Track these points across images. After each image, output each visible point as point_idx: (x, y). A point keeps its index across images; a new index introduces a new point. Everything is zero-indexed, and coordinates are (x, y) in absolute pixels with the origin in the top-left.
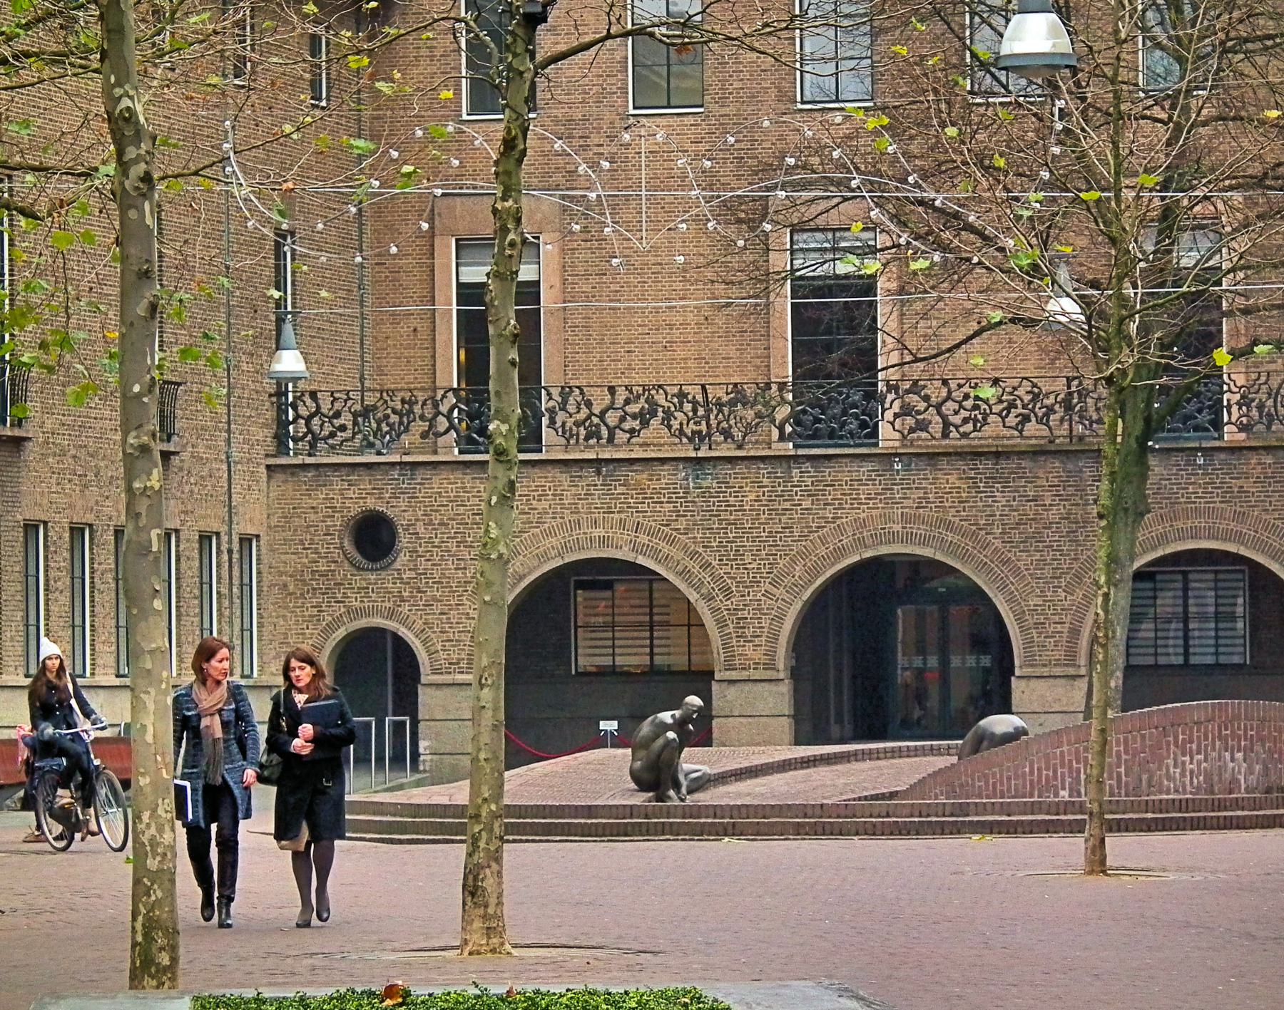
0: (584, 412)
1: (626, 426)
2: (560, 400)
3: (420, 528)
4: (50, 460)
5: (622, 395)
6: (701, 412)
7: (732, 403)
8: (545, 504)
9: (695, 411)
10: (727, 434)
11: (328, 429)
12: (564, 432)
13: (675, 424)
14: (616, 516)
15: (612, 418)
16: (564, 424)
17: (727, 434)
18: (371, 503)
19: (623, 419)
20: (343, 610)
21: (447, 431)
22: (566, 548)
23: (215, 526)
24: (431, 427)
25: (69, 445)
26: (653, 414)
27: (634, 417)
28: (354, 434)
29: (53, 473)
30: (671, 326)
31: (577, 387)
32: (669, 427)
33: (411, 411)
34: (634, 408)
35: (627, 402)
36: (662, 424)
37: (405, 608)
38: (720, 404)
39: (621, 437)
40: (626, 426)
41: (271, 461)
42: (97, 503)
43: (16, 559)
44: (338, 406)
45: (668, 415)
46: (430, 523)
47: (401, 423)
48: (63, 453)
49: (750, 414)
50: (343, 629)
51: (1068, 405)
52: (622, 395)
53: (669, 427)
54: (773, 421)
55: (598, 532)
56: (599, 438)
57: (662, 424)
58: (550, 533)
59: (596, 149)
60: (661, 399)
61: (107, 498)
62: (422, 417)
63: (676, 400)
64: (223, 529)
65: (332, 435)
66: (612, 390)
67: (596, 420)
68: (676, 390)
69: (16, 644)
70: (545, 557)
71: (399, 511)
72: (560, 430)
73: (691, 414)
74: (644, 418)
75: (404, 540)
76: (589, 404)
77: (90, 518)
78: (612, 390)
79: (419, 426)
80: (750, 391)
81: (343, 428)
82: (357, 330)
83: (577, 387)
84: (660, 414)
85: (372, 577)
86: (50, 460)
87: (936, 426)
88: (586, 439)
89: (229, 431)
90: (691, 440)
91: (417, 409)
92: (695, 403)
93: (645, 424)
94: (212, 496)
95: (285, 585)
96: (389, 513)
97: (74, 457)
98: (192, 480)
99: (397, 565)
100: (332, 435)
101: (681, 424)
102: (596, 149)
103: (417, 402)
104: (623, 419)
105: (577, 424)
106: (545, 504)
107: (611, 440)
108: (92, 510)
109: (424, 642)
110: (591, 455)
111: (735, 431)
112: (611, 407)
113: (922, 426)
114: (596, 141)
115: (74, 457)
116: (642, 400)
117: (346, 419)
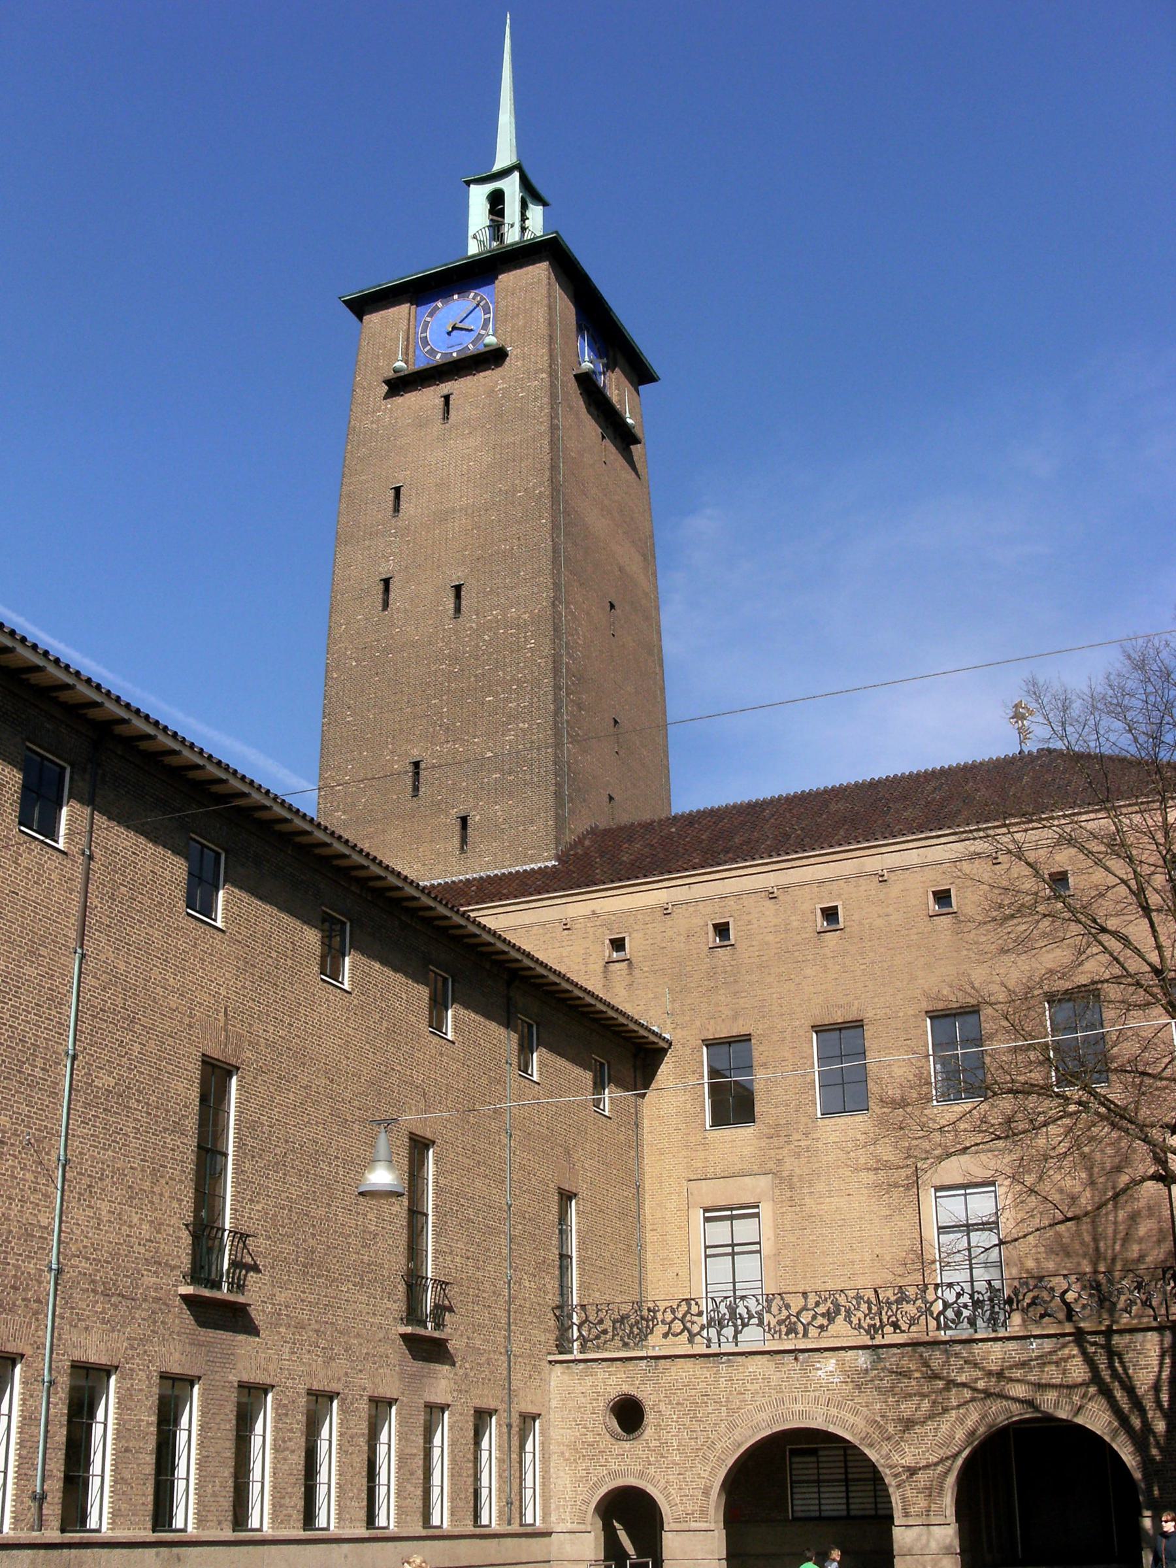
0: (785, 1313)
1: (817, 1323)
2: (765, 1304)
3: (662, 1407)
4: (283, 1330)
6: (874, 1309)
7: (898, 1302)
8: (757, 1386)
9: (870, 1309)
10: (895, 1325)
11: (594, 1332)
12: (770, 1329)
13: (855, 1321)
14: (812, 1394)
15: (806, 1318)
16: (769, 1324)
17: (895, 1325)
18: (626, 1389)
19: (814, 1317)
20: (605, 1472)
21: (682, 1331)
22: (774, 1420)
23: (491, 1404)
24: (670, 1328)
25: (309, 1319)
26: (838, 1312)
27: (823, 1315)
28: (613, 1336)
29: (285, 1342)
30: (853, 1262)
31: (779, 1294)
32: (851, 1323)
33: (654, 1317)
34: (821, 1309)
35: (817, 1304)
36: (845, 1320)
37: (652, 1470)
38: (889, 1303)
39: (813, 1332)
40: (817, 1323)
41: (551, 1358)
42: (346, 1374)
43: (225, 1417)
44: (601, 1315)
46: (670, 1403)
47: (648, 1327)
48: (301, 1326)
49: (910, 1309)
50: (605, 1486)
53: (851, 1323)
54: (931, 1314)
55: (798, 1407)
56: (796, 1333)
57: (845, 1320)
58: (760, 1409)
59: (796, 1144)
60: (842, 1300)
61: (361, 1371)
62: (663, 1322)
63: (854, 1302)
65: (597, 1337)
66: (805, 1294)
67: (794, 1319)
68: (851, 1294)
69: (222, 1499)
70: (757, 1428)
71: (648, 1396)
72: (767, 1328)
73: (867, 1312)
74: (830, 1316)
75: (650, 1417)
76: (788, 1307)
77: (334, 1386)
78: (805, 1294)
79: (661, 1329)
80: (911, 1292)
81: (605, 1332)
82: (636, 1274)
83: (779, 1294)
84: (843, 1314)
85: (627, 1445)
86: (283, 1330)
88: (787, 1334)
89: (509, 1330)
90: (868, 1332)
91: (659, 1316)
92: (869, 1302)
93: (831, 1320)
94: (490, 1380)
95: (563, 1453)
96: (639, 1396)
97: (317, 1331)
98: (467, 1365)
99: (646, 1436)
100: (597, 1337)
101: (859, 1320)
102: (796, 1144)
103: (658, 1311)
104: (814, 1317)
105: (780, 1323)
106: (757, 1386)
107: (805, 1335)
108: (339, 1379)
109: (667, 1497)
110: (789, 1346)
111: (901, 1323)
112: (805, 1308)
114: (796, 1138)
115: (317, 1331)
116: (829, 1301)
117: (608, 1324)
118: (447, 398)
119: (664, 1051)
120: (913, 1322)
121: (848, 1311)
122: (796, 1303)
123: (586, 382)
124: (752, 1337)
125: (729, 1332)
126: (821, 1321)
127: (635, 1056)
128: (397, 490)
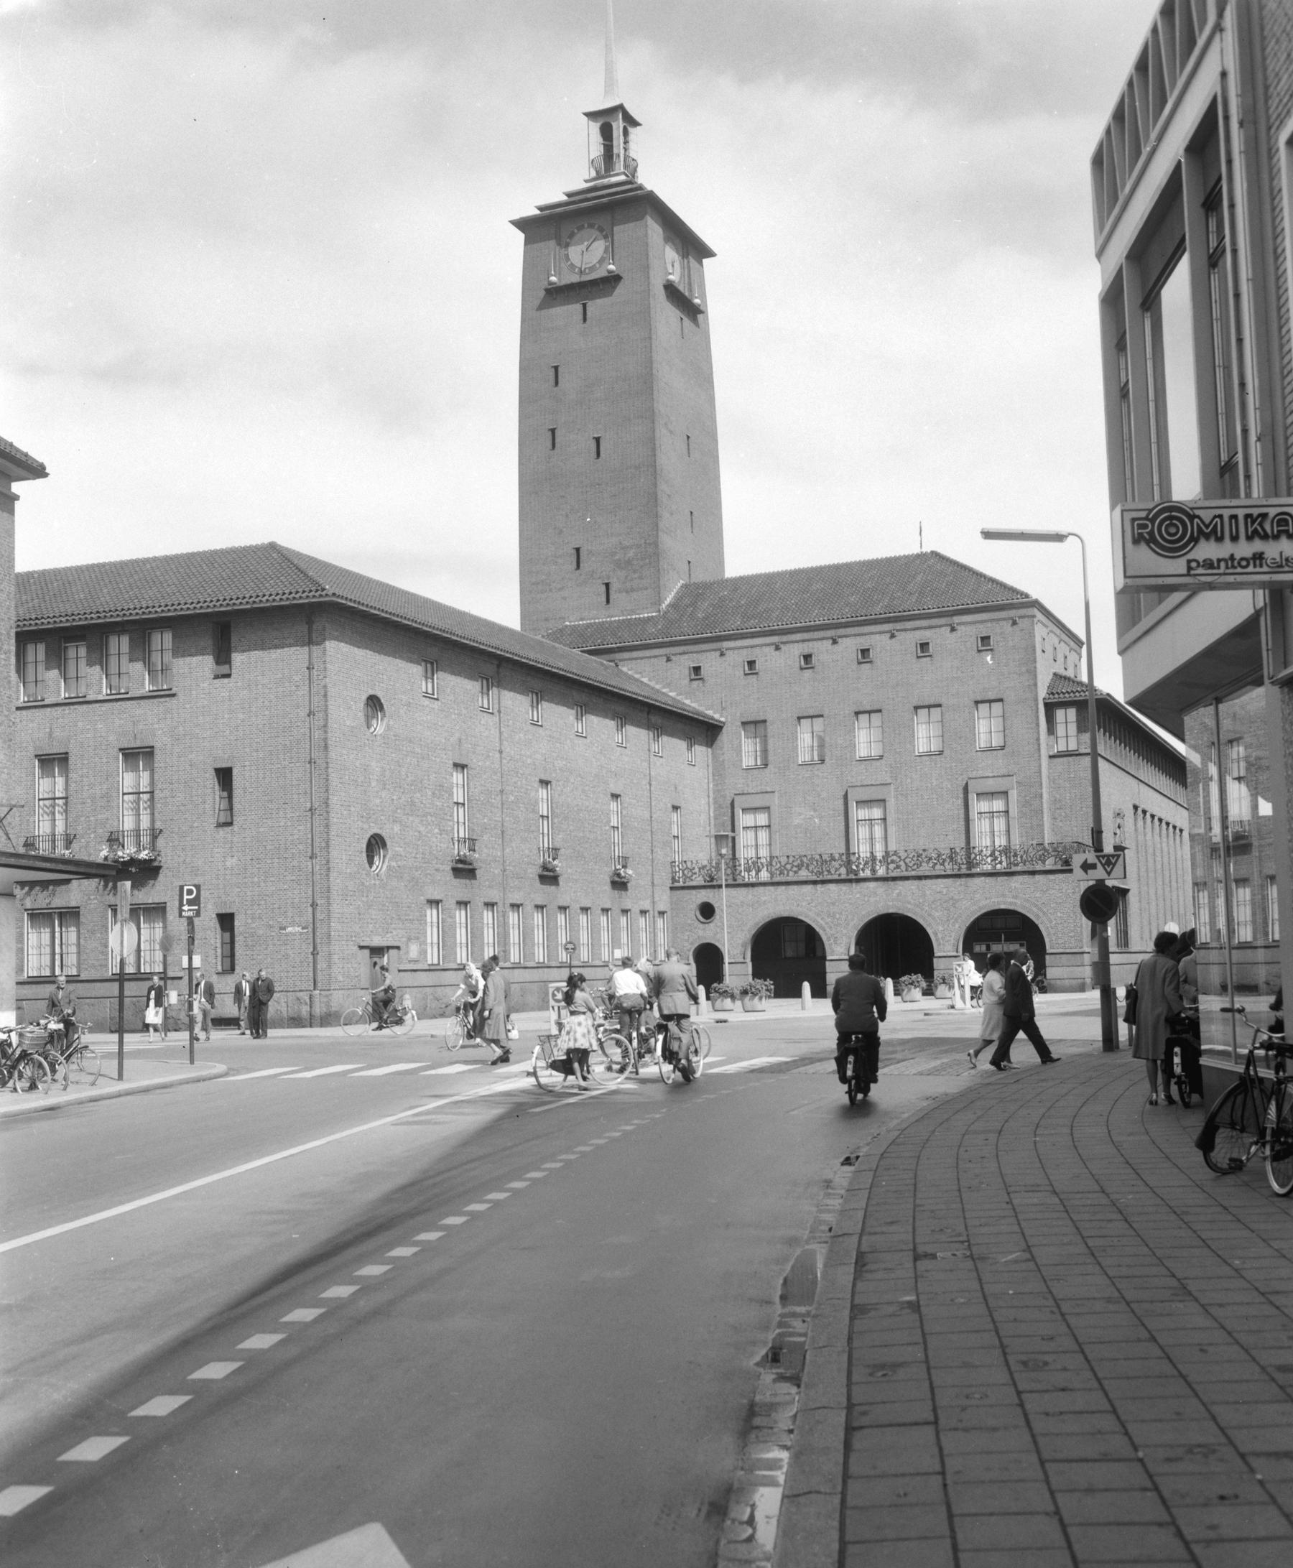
5: (791, 859)
10: (829, 871)
18: (705, 900)
34: (795, 864)
38: (826, 861)
39: (791, 873)
45: (808, 865)
51: (951, 859)
52: (791, 859)
60: (805, 859)
64: (651, 909)
74: (799, 867)
80: (837, 856)
87: (903, 867)
96: (710, 901)
113: (898, 867)
117: (696, 870)
118: (584, 306)
119: (722, 727)
120: (837, 870)
121: (808, 865)
122: (784, 860)
123: (672, 292)
124: (764, 876)
125: (753, 873)
126: (795, 869)
127: (707, 730)
128: (556, 368)
